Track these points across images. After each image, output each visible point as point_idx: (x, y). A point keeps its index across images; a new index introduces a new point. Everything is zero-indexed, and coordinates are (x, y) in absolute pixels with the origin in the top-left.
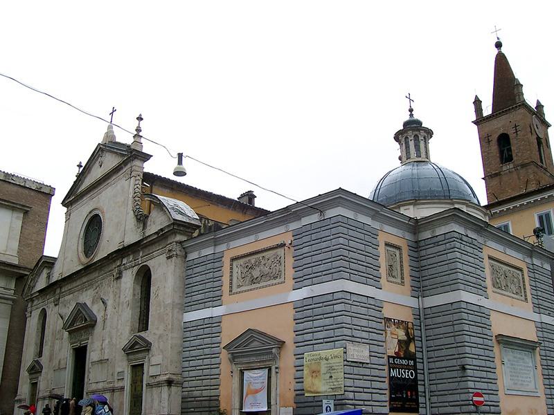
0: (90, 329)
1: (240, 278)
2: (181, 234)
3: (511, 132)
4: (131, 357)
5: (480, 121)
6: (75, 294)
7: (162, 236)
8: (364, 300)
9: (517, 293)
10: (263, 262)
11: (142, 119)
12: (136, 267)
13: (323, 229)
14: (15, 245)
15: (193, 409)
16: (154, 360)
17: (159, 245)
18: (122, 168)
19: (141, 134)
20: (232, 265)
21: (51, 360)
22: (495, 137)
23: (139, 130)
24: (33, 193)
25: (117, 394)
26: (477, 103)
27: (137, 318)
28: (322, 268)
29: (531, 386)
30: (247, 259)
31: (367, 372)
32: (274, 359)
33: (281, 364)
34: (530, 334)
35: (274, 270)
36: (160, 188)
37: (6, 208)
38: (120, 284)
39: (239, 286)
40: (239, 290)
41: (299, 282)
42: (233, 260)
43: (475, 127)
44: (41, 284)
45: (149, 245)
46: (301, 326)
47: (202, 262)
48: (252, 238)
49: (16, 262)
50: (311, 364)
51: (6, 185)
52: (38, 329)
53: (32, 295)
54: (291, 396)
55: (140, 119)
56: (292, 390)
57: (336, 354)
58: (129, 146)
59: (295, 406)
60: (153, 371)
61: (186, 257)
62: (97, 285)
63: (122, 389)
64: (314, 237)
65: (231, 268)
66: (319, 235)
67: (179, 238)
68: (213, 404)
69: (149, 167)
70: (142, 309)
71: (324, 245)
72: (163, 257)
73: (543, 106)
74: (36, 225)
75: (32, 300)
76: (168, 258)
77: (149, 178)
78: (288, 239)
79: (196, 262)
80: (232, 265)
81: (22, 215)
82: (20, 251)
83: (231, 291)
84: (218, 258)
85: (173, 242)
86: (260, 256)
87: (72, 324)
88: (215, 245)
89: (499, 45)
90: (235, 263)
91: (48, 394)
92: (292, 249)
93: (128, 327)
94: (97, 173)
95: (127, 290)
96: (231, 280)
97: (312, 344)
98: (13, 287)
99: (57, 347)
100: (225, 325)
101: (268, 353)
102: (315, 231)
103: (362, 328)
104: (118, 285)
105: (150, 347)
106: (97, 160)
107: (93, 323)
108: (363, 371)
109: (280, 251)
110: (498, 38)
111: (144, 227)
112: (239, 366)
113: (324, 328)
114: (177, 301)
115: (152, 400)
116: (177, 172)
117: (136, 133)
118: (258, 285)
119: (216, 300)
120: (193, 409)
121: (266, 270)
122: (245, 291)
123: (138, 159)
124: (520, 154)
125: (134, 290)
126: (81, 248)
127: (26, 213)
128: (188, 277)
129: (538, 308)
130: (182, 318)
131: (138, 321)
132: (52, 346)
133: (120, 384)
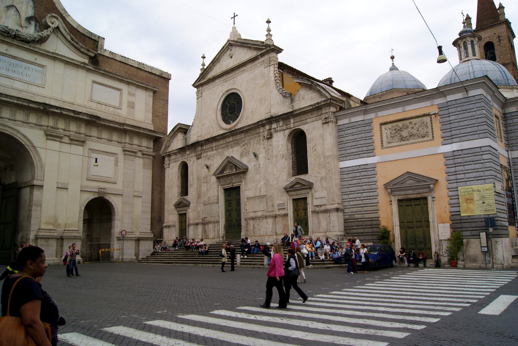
0: (242, 175)
1: (389, 137)
2: (333, 106)
3: (495, 41)
4: (291, 193)
6: (220, 150)
7: (316, 108)
10: (410, 126)
11: (270, 22)
12: (288, 130)
13: (467, 103)
15: (356, 227)
16: (316, 195)
17: (312, 114)
18: (258, 59)
19: (271, 33)
20: (381, 128)
21: (199, 197)
23: (269, 30)
24: (157, 78)
25: (279, 219)
26: (468, 18)
27: (291, 165)
28: (469, 130)
30: (395, 124)
32: (431, 190)
33: (436, 194)
35: (422, 131)
36: (287, 74)
37: (142, 89)
38: (272, 142)
39: (389, 143)
40: (389, 145)
42: (382, 124)
44: (178, 143)
45: (301, 115)
47: (353, 126)
48: (400, 109)
49: (152, 129)
50: (465, 194)
51: (139, 71)
52: (178, 176)
53: (170, 152)
54: (447, 216)
55: (268, 22)
56: (448, 211)
57: (487, 188)
58: (263, 42)
59: (451, 222)
60: (316, 202)
61: (337, 123)
62: (244, 143)
63: (286, 215)
64: (459, 109)
65: (381, 131)
66: (464, 108)
67: (333, 109)
68: (375, 223)
69: (282, 58)
70: (294, 160)
71: (470, 114)
72: (320, 122)
73: (511, 23)
74: (161, 101)
75: (169, 156)
76: (324, 124)
77: (282, 66)
79: (346, 126)
80: (381, 128)
81: (152, 94)
82: (153, 121)
83: (382, 146)
84: (370, 123)
85: (329, 112)
86: (407, 122)
87: (222, 171)
88: (364, 114)
90: (383, 127)
91: (201, 221)
92: (439, 117)
93: (285, 173)
94: (227, 63)
95: (280, 147)
96: (382, 138)
97: (466, 181)
98: (152, 146)
99: (204, 188)
100: (378, 170)
101: (427, 188)
102: (460, 105)
104: (270, 143)
105: (313, 186)
106: (225, 53)
107: (245, 170)
109: (427, 119)
111: (292, 101)
112: (396, 197)
113: (475, 170)
114: (336, 153)
115: (319, 223)
116: (439, 61)
117: (267, 33)
118: (407, 142)
119: (370, 152)
120: (356, 227)
121: (414, 131)
122: (396, 146)
123: (274, 52)
124: (502, 57)
125: (287, 146)
126: (220, 117)
127: (155, 92)
128: (339, 137)
130: (339, 165)
131: (291, 168)
132: (199, 188)
133: (282, 212)
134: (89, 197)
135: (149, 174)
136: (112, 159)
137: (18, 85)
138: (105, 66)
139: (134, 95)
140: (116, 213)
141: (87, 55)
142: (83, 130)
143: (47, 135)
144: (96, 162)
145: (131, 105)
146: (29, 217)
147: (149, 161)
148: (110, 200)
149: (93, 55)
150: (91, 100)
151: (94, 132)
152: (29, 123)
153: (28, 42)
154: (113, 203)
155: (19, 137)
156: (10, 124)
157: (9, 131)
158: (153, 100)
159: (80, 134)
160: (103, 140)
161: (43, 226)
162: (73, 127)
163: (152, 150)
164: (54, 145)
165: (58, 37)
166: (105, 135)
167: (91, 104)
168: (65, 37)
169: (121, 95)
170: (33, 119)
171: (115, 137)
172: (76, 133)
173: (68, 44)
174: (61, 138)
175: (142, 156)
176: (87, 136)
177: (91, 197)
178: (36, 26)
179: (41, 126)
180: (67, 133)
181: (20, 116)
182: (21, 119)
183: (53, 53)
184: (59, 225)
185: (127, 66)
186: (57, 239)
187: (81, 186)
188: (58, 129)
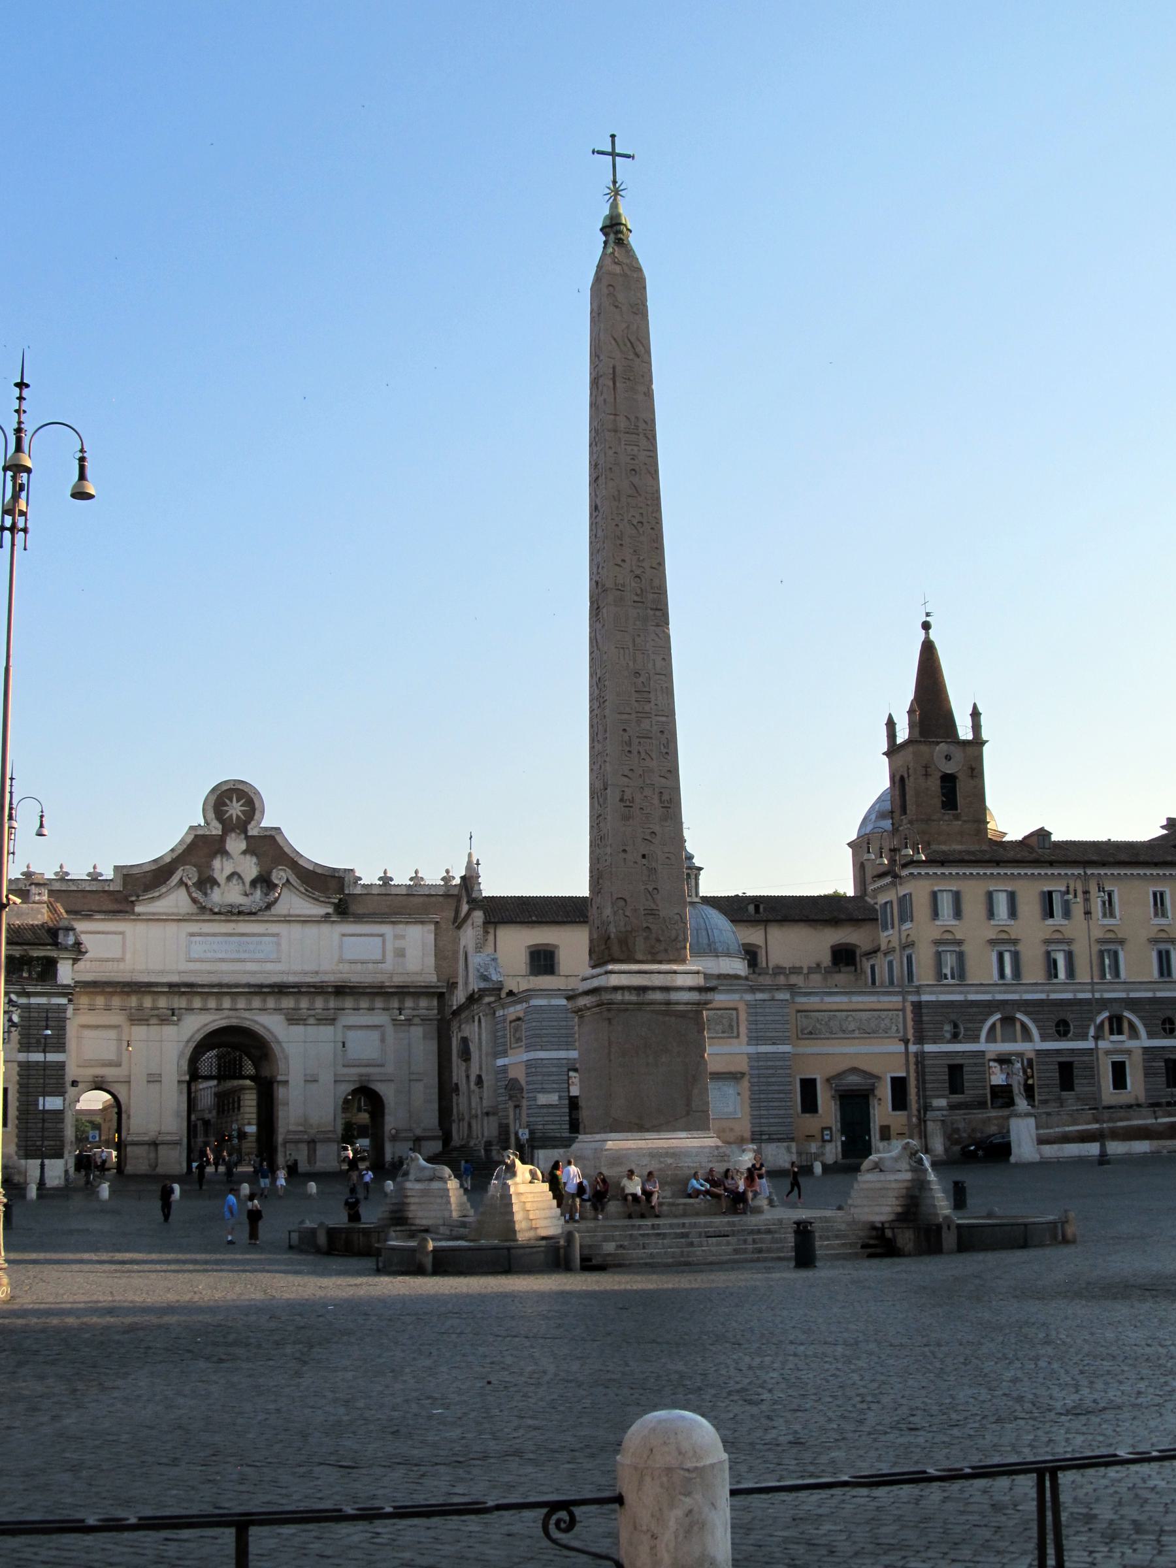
3: (906, 776)
5: (893, 750)
8: (555, 1061)
9: (723, 1032)
14: (431, 961)
22: (897, 778)
26: (891, 724)
29: (731, 1109)
31: (557, 1110)
34: (743, 1065)
41: (530, 1047)
42: (511, 1022)
43: (886, 759)
46: (530, 1079)
51: (411, 899)
61: (494, 1014)
78: (521, 1015)
82: (438, 968)
89: (926, 626)
103: (554, 1082)
108: (551, 1110)
110: (928, 615)
119: (504, 1053)
129: (755, 1038)
134: (346, 1088)
135: (433, 1046)
136: (375, 1035)
137: (250, 967)
138: (355, 908)
139: (403, 937)
140: (387, 1106)
141: (329, 903)
142: (332, 1004)
143: (288, 1020)
144: (344, 1046)
145: (400, 953)
146: (278, 1118)
147: (433, 1028)
148: (377, 1089)
149: (336, 901)
150: (341, 961)
151: (349, 1003)
152: (265, 1010)
153: (254, 914)
154: (381, 1094)
155: (256, 1028)
156: (247, 1015)
157: (246, 1024)
158: (436, 935)
159: (329, 1009)
160: (362, 1011)
161: (292, 1128)
162: (319, 1003)
163: (435, 1012)
164: (299, 1029)
165: (289, 890)
166: (364, 1003)
167: (341, 966)
168: (298, 890)
169: (384, 942)
170: (271, 1003)
171: (379, 1003)
172: (324, 1009)
173: (303, 896)
174: (305, 1020)
175: (420, 1022)
176: (338, 1009)
177: (352, 1087)
178: (261, 887)
179: (281, 1009)
180: (312, 1012)
181: (256, 1002)
182: (257, 1007)
183: (285, 916)
184: (311, 1126)
185: (390, 898)
186: (309, 1142)
187: (335, 1075)
188: (300, 1009)
